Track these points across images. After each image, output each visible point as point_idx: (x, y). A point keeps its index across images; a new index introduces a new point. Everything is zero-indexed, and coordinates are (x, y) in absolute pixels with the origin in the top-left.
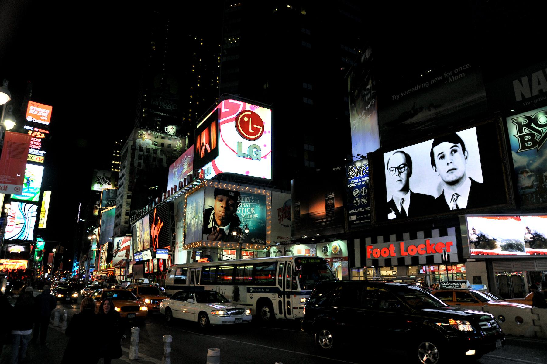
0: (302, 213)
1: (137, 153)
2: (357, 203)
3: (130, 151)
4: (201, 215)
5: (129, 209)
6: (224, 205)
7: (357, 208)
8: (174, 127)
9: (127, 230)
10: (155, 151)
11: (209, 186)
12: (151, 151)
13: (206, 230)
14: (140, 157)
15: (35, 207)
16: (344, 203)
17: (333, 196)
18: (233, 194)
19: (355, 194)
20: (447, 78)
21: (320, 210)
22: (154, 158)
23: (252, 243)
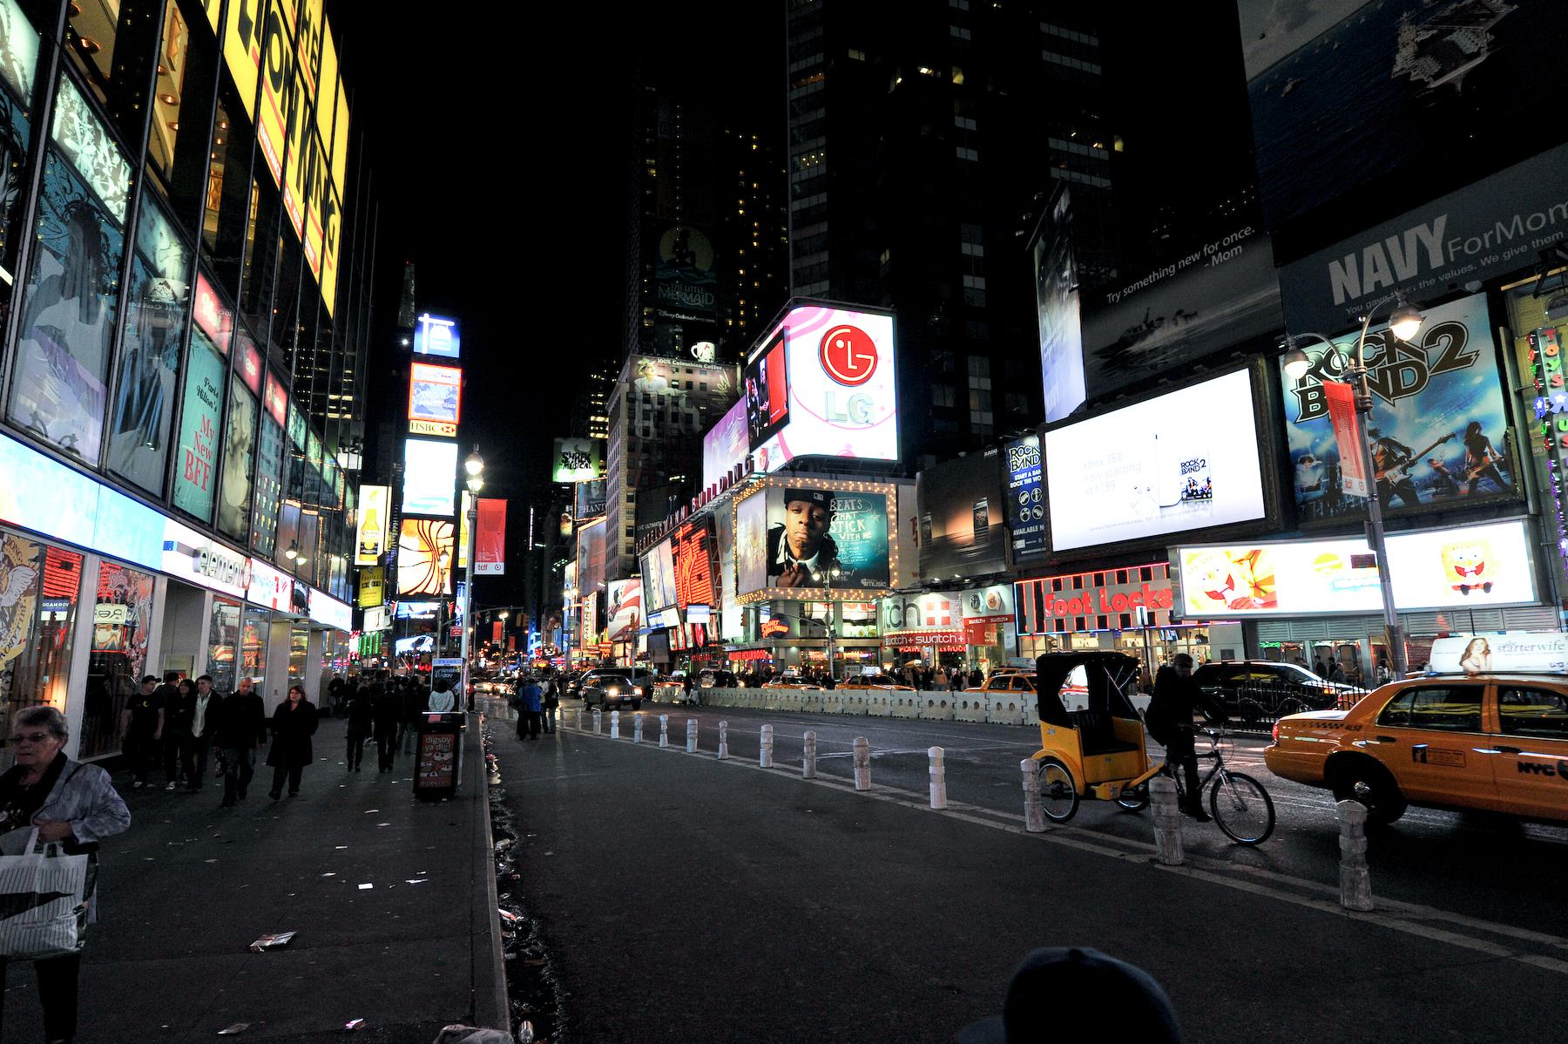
0: (936, 535)
1: (640, 407)
2: (1025, 516)
3: (624, 404)
4: (762, 541)
5: (632, 522)
6: (805, 520)
8: (711, 346)
9: (632, 568)
10: (675, 401)
11: (776, 486)
12: (668, 401)
13: (773, 569)
15: (449, 528)
16: (1005, 517)
17: (984, 504)
18: (820, 498)
19: (1022, 500)
20: (1210, 256)
21: (963, 529)
22: (675, 416)
23: (863, 587)
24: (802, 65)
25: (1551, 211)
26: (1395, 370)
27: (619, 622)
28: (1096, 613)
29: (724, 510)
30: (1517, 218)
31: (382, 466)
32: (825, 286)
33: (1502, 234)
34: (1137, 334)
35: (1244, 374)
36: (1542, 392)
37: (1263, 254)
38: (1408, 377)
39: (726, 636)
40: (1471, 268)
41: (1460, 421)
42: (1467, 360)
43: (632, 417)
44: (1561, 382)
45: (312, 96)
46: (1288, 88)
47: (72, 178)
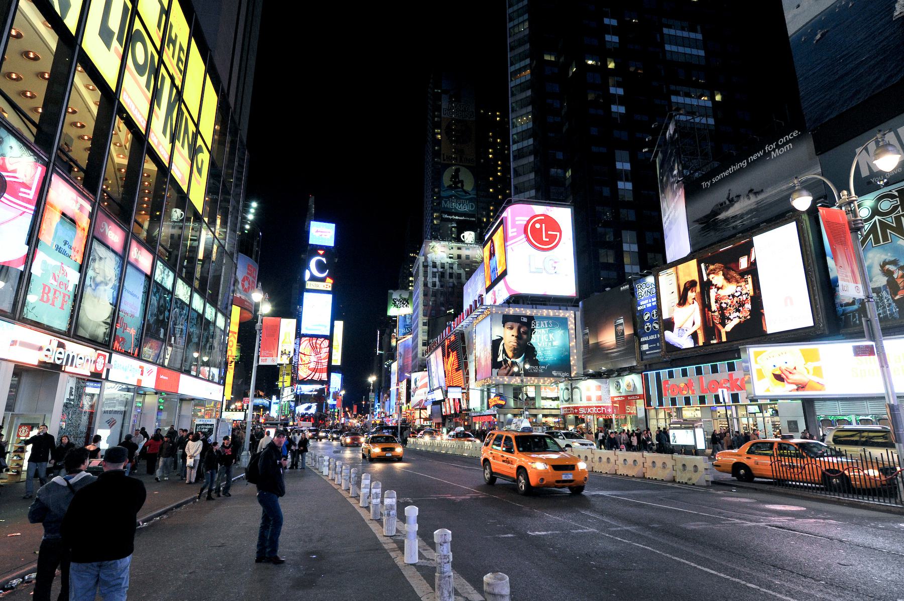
0: (592, 342)
1: (430, 270)
2: (648, 329)
3: (421, 269)
5: (426, 338)
6: (515, 334)
7: (649, 335)
8: (473, 234)
9: (423, 366)
11: (497, 313)
12: (447, 266)
13: (496, 364)
16: (635, 330)
17: (622, 321)
18: (525, 320)
19: (646, 318)
20: (770, 152)
21: (608, 338)
22: (451, 275)
23: (553, 376)
24: (517, 66)
28: (698, 393)
29: (469, 329)
31: (289, 304)
32: (533, 193)
34: (723, 207)
35: (793, 226)
37: (807, 148)
39: (471, 407)
43: (426, 276)
45: (178, 83)
46: (818, 36)
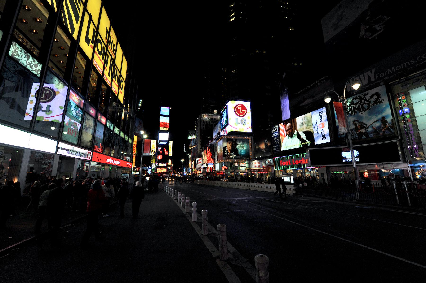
0: (257, 147)
1: (202, 123)
3: (199, 123)
4: (222, 149)
7: (276, 145)
9: (200, 156)
10: (209, 122)
12: (208, 122)
13: (224, 155)
14: (203, 125)
18: (234, 140)
21: (263, 146)
25: (402, 65)
26: (362, 105)
27: (198, 167)
30: (393, 68)
31: (153, 135)
32: (237, 97)
33: (390, 72)
36: (401, 108)
38: (366, 107)
40: (382, 80)
41: (380, 116)
42: (381, 102)
43: (201, 126)
44: (406, 106)
45: (113, 57)
47: (18, 65)
